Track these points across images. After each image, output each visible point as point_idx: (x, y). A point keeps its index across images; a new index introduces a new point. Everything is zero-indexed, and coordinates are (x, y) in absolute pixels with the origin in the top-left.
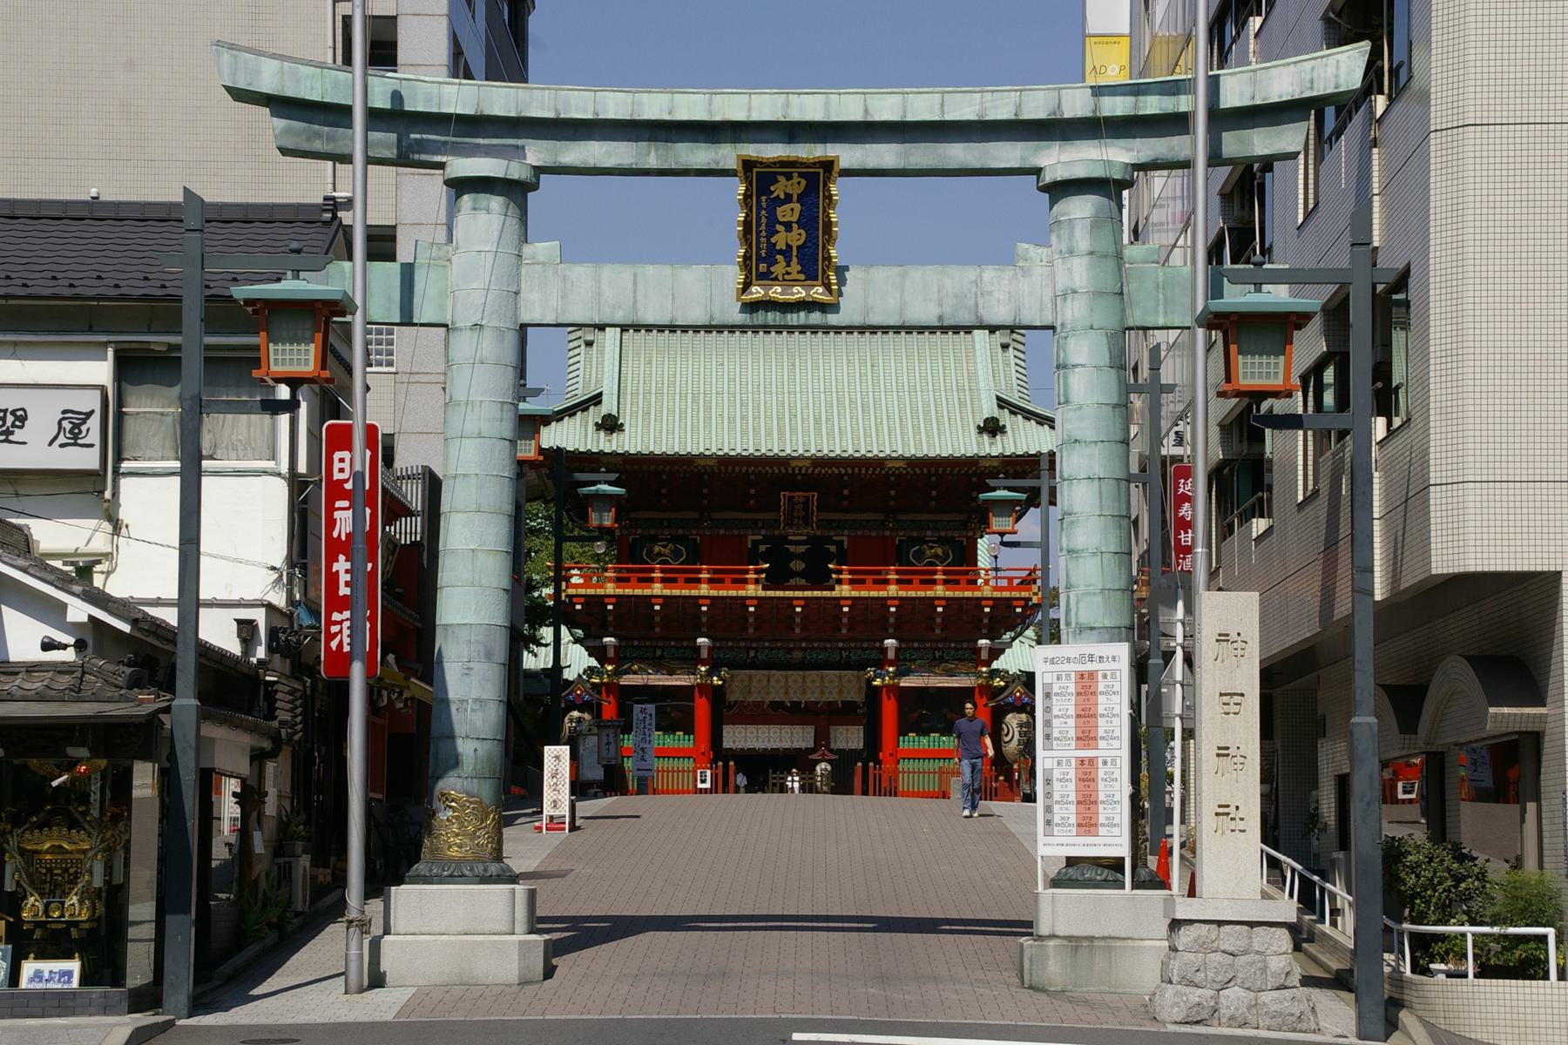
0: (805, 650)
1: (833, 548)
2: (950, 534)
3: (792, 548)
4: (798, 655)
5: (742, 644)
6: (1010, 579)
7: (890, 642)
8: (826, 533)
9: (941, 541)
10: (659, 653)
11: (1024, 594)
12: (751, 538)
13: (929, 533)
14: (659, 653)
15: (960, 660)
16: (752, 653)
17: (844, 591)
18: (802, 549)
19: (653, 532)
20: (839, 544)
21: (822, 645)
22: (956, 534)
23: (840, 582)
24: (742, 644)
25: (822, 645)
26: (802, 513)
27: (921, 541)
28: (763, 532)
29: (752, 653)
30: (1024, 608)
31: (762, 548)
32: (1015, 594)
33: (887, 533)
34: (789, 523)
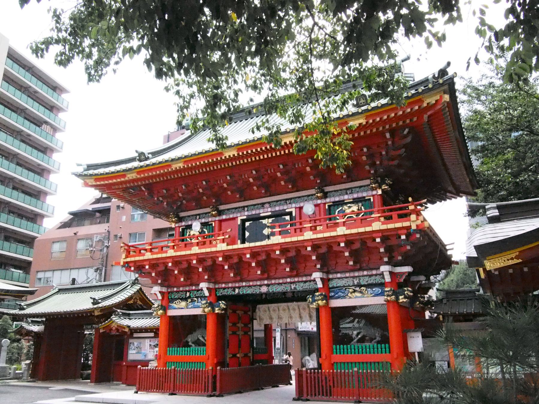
0: (268, 285)
1: (288, 218)
2: (360, 195)
3: (265, 221)
4: (264, 289)
5: (230, 285)
8: (281, 208)
9: (355, 201)
10: (188, 294)
12: (239, 219)
13: (346, 197)
14: (188, 294)
16: (237, 291)
18: (270, 220)
20: (290, 214)
22: (365, 194)
23: (273, 234)
24: (230, 285)
27: (342, 203)
28: (246, 213)
31: (247, 224)
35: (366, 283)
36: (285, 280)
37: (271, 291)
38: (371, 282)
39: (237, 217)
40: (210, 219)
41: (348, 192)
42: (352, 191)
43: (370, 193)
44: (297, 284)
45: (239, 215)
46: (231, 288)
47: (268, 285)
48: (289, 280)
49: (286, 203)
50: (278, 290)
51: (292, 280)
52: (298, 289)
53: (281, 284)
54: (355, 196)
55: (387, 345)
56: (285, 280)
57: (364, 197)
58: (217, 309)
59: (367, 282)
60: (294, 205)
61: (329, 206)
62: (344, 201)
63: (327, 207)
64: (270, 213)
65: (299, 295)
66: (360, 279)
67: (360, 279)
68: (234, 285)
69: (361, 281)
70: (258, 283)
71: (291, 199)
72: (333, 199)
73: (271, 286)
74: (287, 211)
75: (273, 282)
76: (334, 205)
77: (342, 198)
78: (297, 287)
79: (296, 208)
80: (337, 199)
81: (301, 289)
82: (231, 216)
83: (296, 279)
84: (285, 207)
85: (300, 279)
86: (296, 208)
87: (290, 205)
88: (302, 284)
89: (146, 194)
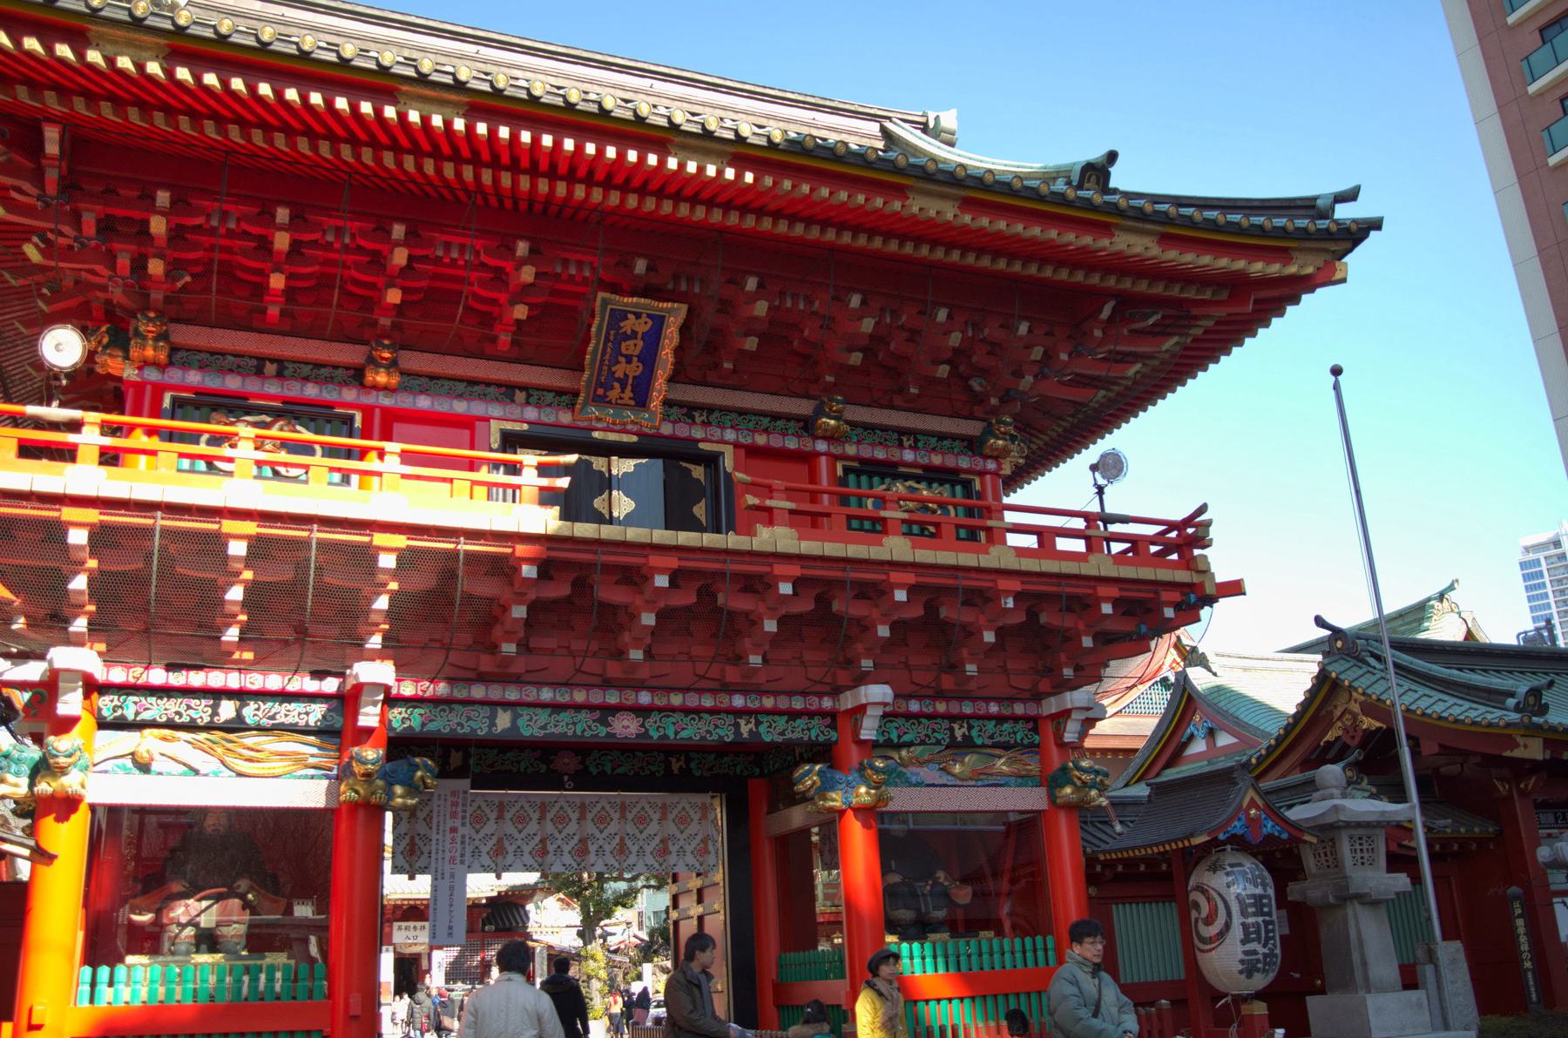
0: (642, 711)
1: (698, 472)
2: (950, 462)
4: (626, 727)
5: (478, 692)
6: (1136, 542)
7: (878, 693)
8: (683, 431)
9: (932, 475)
11: (1182, 576)
12: (495, 426)
14: (227, 710)
15: (1006, 747)
17: (776, 538)
19: (233, 383)
20: (711, 461)
21: (692, 700)
22: (964, 463)
23: (768, 516)
24: (478, 692)
25: (692, 700)
26: (635, 369)
28: (531, 413)
29: (503, 720)
30: (1177, 607)
32: (1164, 575)
33: (821, 446)
34: (600, 400)
35: (988, 742)
36: (724, 701)
37: (655, 735)
38: (1002, 739)
39: (487, 419)
40: (350, 395)
41: (906, 444)
42: (916, 441)
43: (980, 464)
44: (764, 718)
45: (495, 410)
46: (483, 703)
47: (642, 711)
48: (738, 701)
49: (693, 418)
50: (684, 734)
51: (753, 704)
52: (768, 738)
53: (699, 711)
54: (937, 460)
55: (1050, 939)
56: (724, 701)
57: (956, 471)
58: (399, 790)
59: (991, 737)
60: (730, 435)
61: (847, 470)
62: (895, 465)
63: (840, 472)
64: (635, 439)
65: (608, 769)
66: (970, 728)
67: (970, 728)
68: (495, 692)
69: (974, 733)
70: (613, 698)
71: (711, 409)
72: (866, 452)
73: (655, 716)
74: (702, 445)
75: (676, 700)
76: (858, 473)
77: (895, 454)
78: (762, 729)
79: (737, 445)
80: (880, 454)
81: (780, 739)
82: (460, 407)
83: (768, 702)
84: (698, 433)
85: (783, 703)
86: (737, 445)
87: (716, 433)
88: (781, 721)
89: (52, 174)
